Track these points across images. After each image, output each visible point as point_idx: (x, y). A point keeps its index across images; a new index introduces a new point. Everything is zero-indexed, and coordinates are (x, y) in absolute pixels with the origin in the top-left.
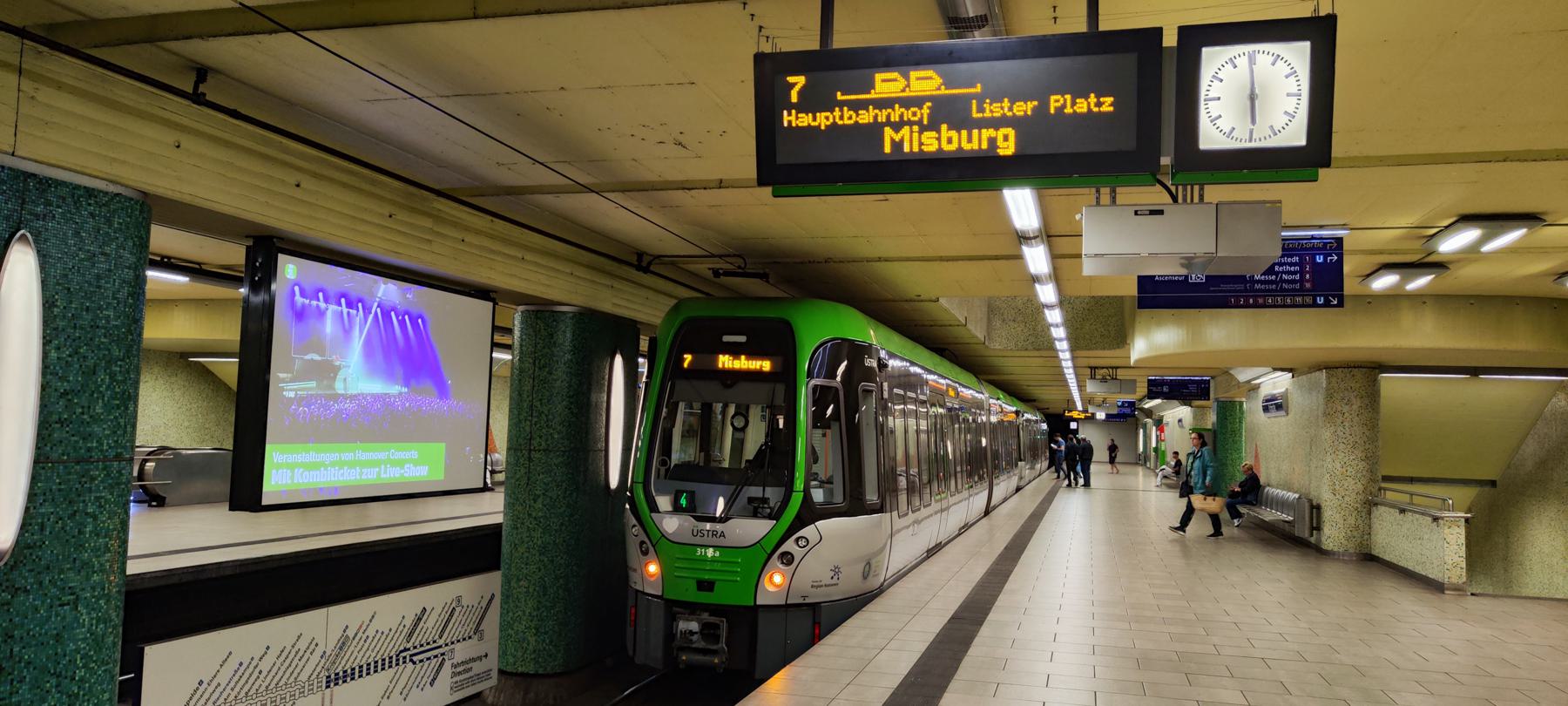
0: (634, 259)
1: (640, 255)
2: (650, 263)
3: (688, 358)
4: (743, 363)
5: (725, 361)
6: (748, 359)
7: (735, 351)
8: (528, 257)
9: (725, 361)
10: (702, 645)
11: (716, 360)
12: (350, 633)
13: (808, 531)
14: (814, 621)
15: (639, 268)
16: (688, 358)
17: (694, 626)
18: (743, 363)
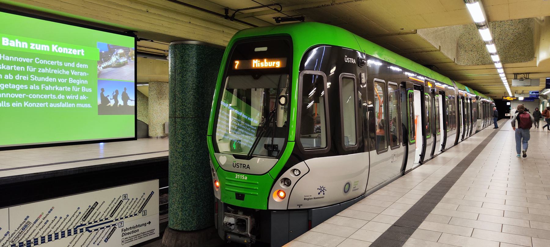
0: (223, 13)
1: (227, 10)
2: (234, 15)
3: (237, 62)
4: (266, 64)
5: (256, 63)
6: (268, 61)
7: (261, 56)
8: (152, 10)
9: (256, 63)
10: (237, 231)
11: (251, 63)
12: (32, 220)
13: (297, 166)
14: (308, 218)
15: (226, 17)
16: (237, 62)
17: (232, 220)
18: (266, 64)
